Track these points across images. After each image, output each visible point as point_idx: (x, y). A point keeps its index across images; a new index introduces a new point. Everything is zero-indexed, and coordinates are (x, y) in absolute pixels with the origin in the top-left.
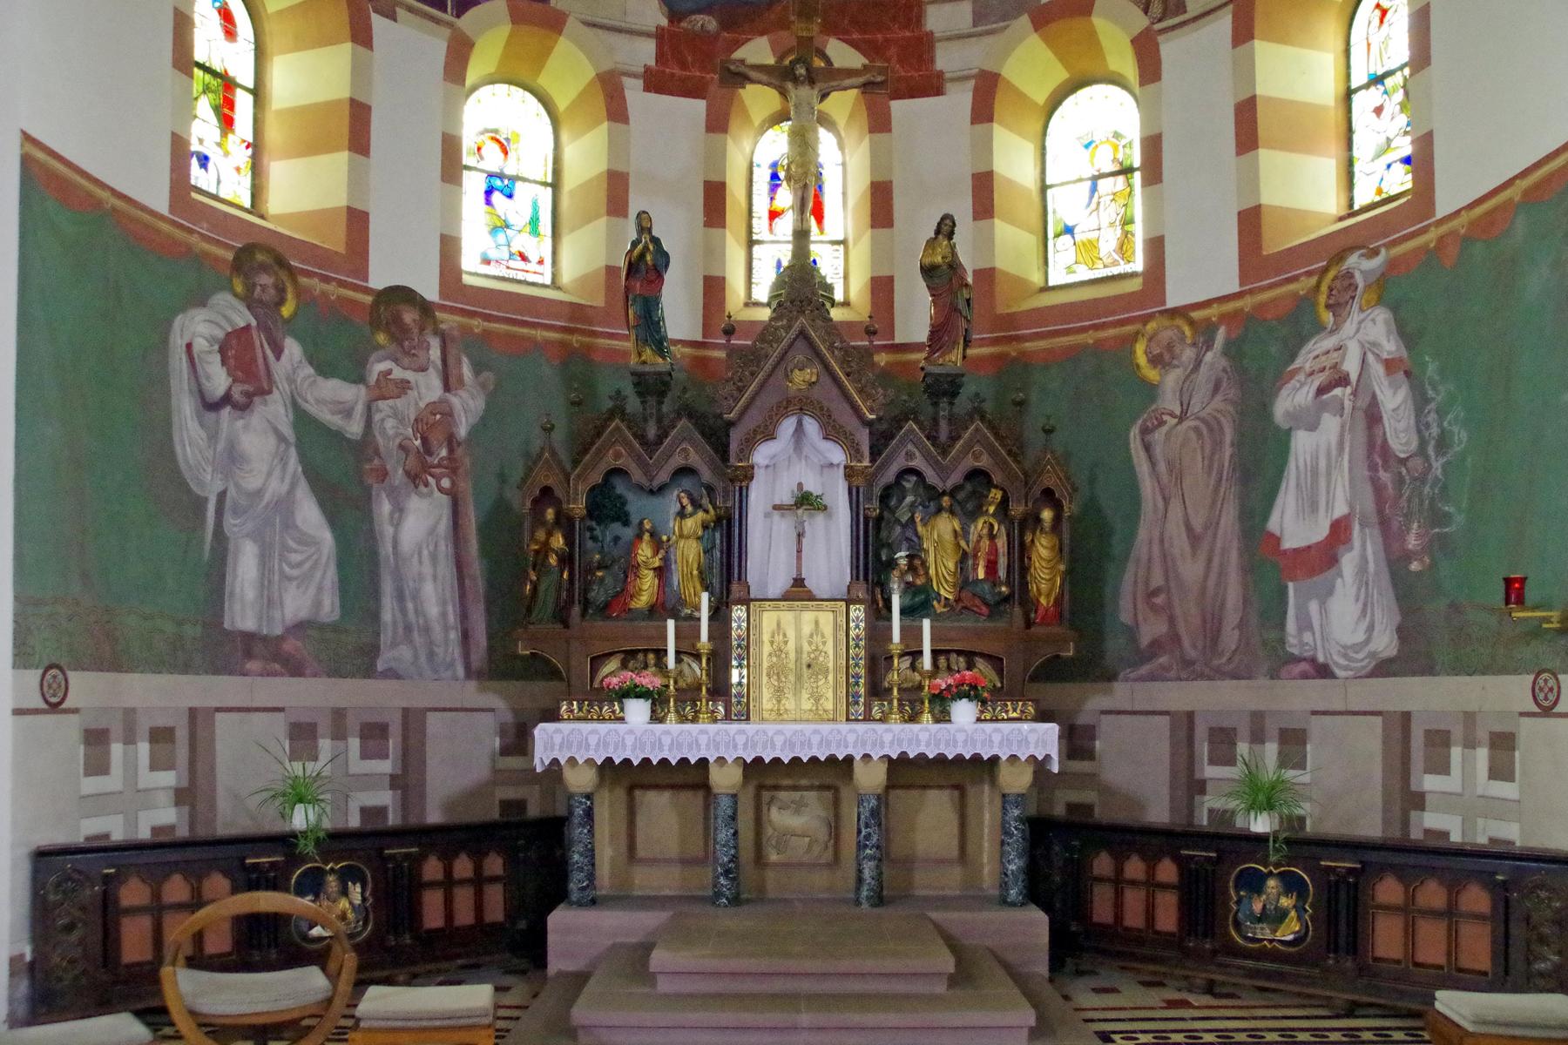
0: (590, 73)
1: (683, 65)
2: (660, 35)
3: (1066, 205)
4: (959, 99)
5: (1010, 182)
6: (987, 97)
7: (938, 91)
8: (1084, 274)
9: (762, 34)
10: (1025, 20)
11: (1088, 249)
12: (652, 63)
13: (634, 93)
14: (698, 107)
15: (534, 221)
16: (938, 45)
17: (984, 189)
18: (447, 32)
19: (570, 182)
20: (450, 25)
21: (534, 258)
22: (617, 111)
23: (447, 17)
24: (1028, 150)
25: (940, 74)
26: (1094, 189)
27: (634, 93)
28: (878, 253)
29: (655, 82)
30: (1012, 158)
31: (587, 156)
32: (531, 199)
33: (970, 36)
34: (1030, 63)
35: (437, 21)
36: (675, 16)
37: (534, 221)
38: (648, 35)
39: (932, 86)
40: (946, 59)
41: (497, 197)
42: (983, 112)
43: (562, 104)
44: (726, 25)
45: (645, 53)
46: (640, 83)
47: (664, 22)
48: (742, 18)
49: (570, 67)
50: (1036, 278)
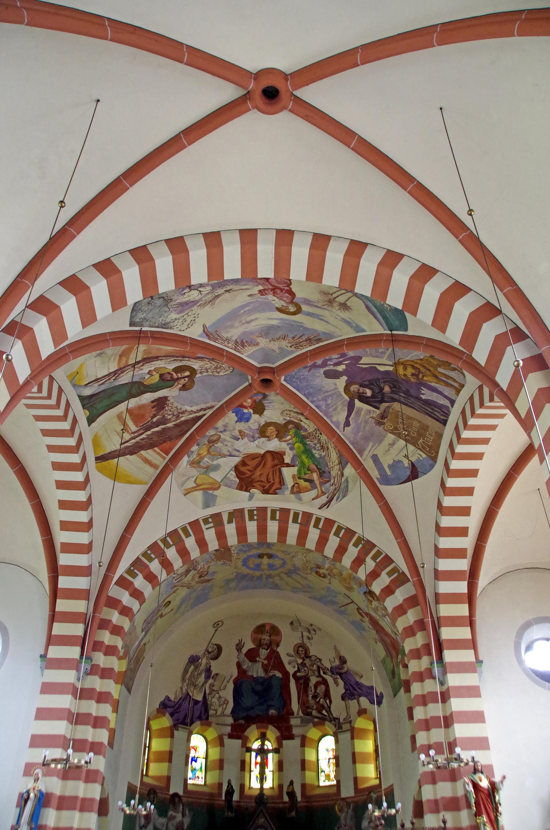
0: (216, 735)
1: (237, 732)
2: (233, 726)
3: (323, 764)
4: (297, 742)
5: (310, 761)
6: (304, 741)
7: (293, 739)
8: (327, 783)
9: (254, 724)
10: (311, 724)
11: (328, 777)
12: (230, 732)
13: (227, 740)
14: (239, 742)
15: (201, 768)
16: (293, 728)
17: (303, 764)
18: (188, 731)
19: (210, 759)
20: (189, 729)
21: (200, 777)
22: (222, 744)
23: (188, 727)
24: (314, 751)
25: (294, 735)
26: (329, 761)
27: (227, 740)
28: (280, 778)
29: (231, 736)
30: (310, 755)
31: (215, 753)
32: (201, 763)
33: (301, 726)
34: (313, 733)
35: (186, 729)
36: (235, 720)
37: (201, 768)
38: (228, 725)
39: (291, 737)
40: (295, 731)
41: (193, 762)
42: (303, 745)
43: (209, 739)
44: (246, 723)
45: (228, 729)
46: (227, 737)
47: (233, 722)
48: (250, 720)
49: (212, 733)
50: (316, 784)
